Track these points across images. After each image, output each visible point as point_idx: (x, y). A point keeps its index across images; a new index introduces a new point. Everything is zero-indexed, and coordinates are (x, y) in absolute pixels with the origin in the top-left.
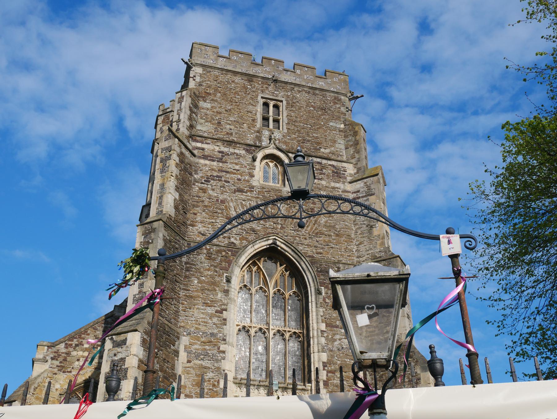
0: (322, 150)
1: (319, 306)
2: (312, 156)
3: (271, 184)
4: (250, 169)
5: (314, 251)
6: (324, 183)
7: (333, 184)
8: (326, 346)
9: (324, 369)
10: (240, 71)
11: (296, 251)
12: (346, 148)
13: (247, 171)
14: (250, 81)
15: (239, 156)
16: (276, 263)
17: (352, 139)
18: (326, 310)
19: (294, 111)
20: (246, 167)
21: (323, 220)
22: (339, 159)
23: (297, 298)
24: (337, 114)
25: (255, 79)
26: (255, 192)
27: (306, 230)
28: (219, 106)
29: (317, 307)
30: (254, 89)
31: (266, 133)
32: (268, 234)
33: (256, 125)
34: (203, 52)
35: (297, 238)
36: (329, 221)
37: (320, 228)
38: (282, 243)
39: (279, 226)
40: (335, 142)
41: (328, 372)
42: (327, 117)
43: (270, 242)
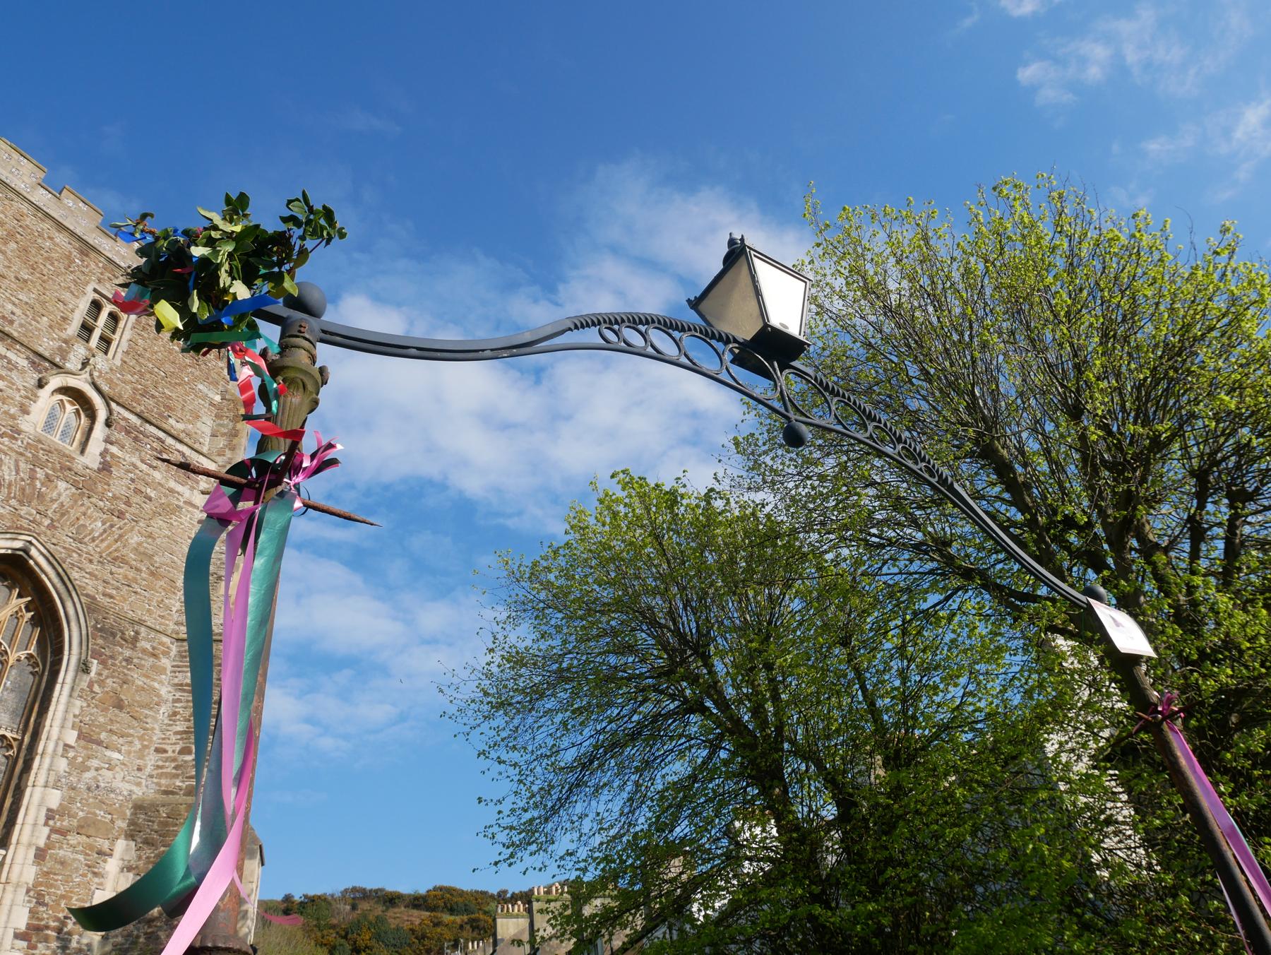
0: (172, 421)
1: (76, 694)
2: (151, 423)
3: (56, 439)
4: (27, 397)
5: (100, 588)
6: (157, 475)
7: (172, 484)
8: (65, 777)
9: (46, 824)
10: (72, 228)
11: (66, 578)
12: (213, 435)
13: (18, 398)
14: (82, 253)
15: (11, 366)
16: (10, 588)
17: (227, 425)
18: (89, 706)
19: (144, 339)
20: (19, 390)
21: (136, 538)
22: (196, 446)
23: (30, 669)
24: (216, 376)
25: (93, 255)
26: (19, 443)
27: (97, 546)
28: (6, 263)
29: (71, 696)
30: (84, 269)
31: (80, 351)
32: (17, 528)
33: (65, 329)
34: (13, 162)
35: (75, 555)
36: (145, 545)
37: (124, 552)
38: (42, 553)
39: (47, 522)
40: (198, 417)
41: (53, 831)
42: (197, 373)
43: (18, 544)
